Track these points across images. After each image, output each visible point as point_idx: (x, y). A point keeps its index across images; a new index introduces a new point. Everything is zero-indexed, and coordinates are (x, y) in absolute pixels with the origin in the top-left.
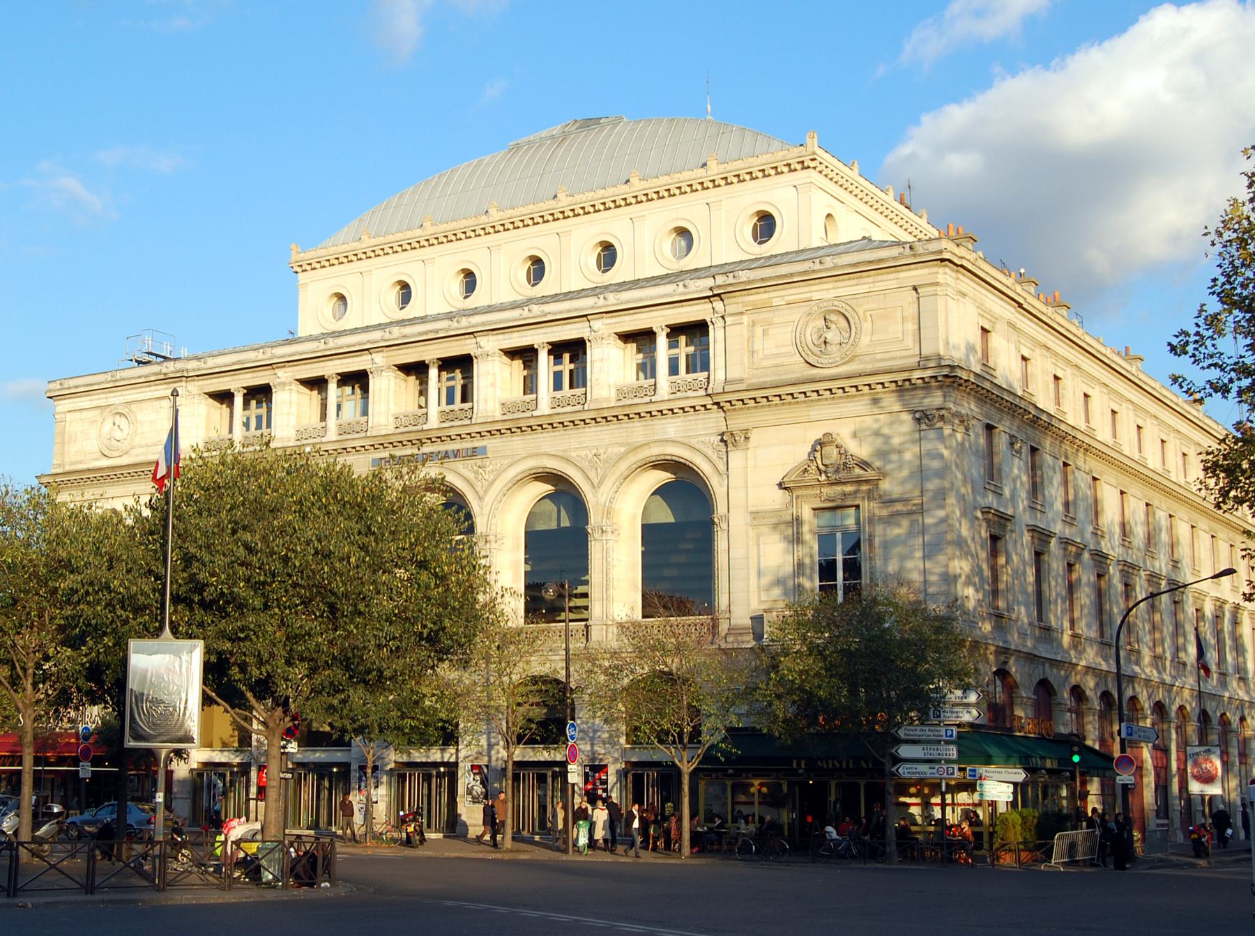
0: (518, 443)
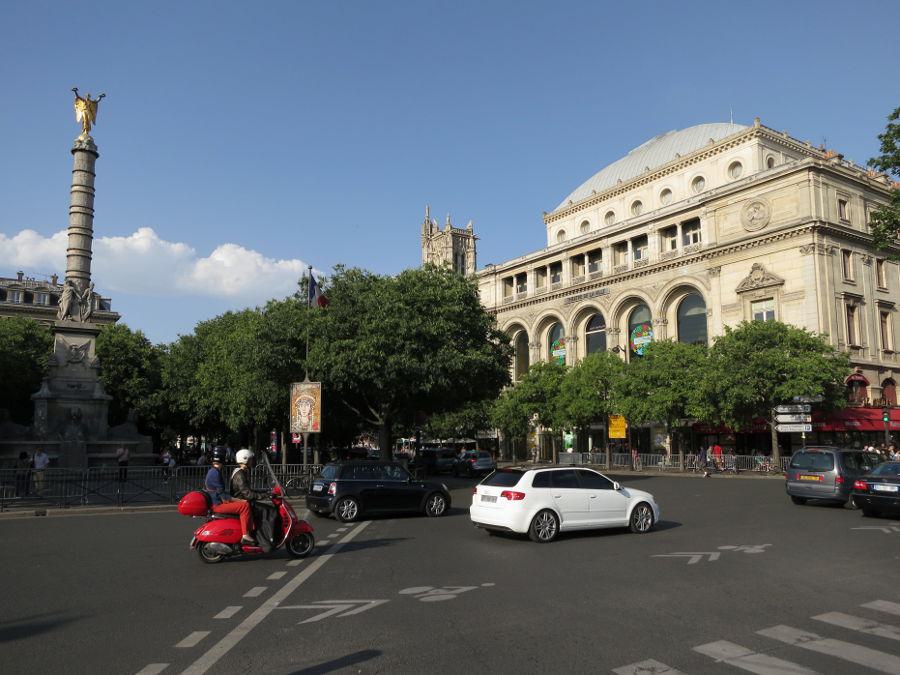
0: (621, 286)
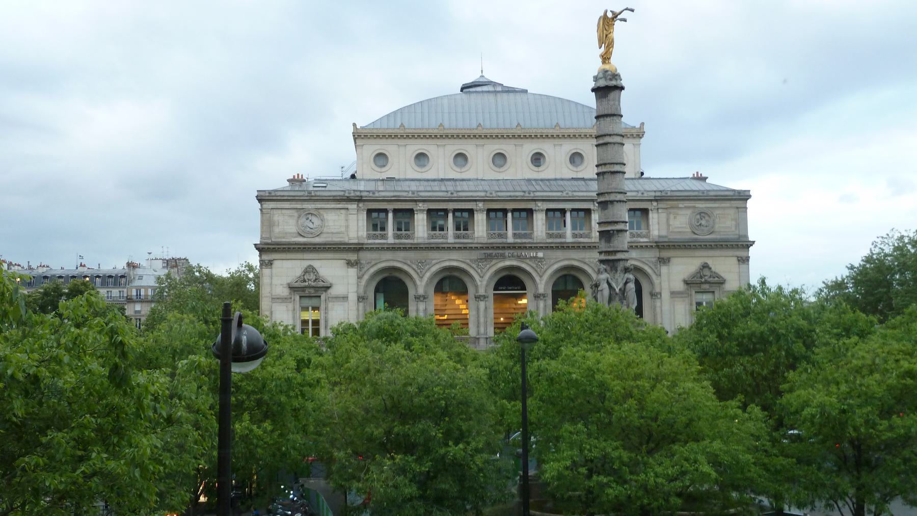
0: (559, 254)
